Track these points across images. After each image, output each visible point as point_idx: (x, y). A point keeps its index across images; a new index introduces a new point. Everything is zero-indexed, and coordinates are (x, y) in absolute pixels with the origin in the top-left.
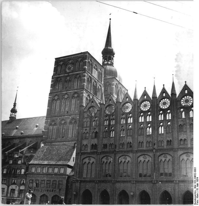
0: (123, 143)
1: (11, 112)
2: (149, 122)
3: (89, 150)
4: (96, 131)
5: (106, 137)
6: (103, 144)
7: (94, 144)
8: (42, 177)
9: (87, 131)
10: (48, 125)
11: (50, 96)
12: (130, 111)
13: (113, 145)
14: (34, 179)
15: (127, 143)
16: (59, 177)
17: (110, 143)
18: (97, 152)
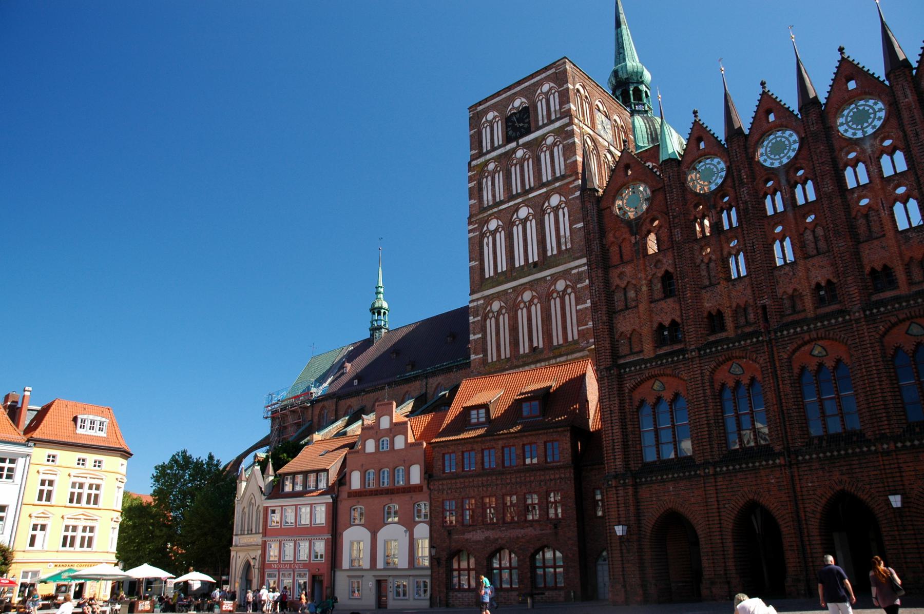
0: (795, 290)
1: (370, 314)
2: (898, 178)
3: (648, 350)
4: (667, 272)
5: (710, 282)
6: (705, 315)
7: (667, 323)
8: (483, 486)
9: (630, 279)
10: (479, 318)
11: (471, 227)
12: (796, 157)
13: (750, 310)
14: (457, 495)
15: (813, 286)
16: (547, 477)
17: (734, 305)
18: (683, 351)
